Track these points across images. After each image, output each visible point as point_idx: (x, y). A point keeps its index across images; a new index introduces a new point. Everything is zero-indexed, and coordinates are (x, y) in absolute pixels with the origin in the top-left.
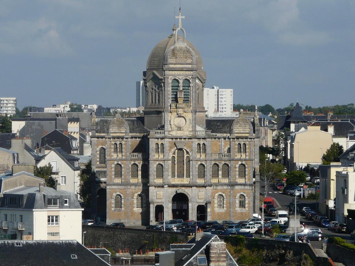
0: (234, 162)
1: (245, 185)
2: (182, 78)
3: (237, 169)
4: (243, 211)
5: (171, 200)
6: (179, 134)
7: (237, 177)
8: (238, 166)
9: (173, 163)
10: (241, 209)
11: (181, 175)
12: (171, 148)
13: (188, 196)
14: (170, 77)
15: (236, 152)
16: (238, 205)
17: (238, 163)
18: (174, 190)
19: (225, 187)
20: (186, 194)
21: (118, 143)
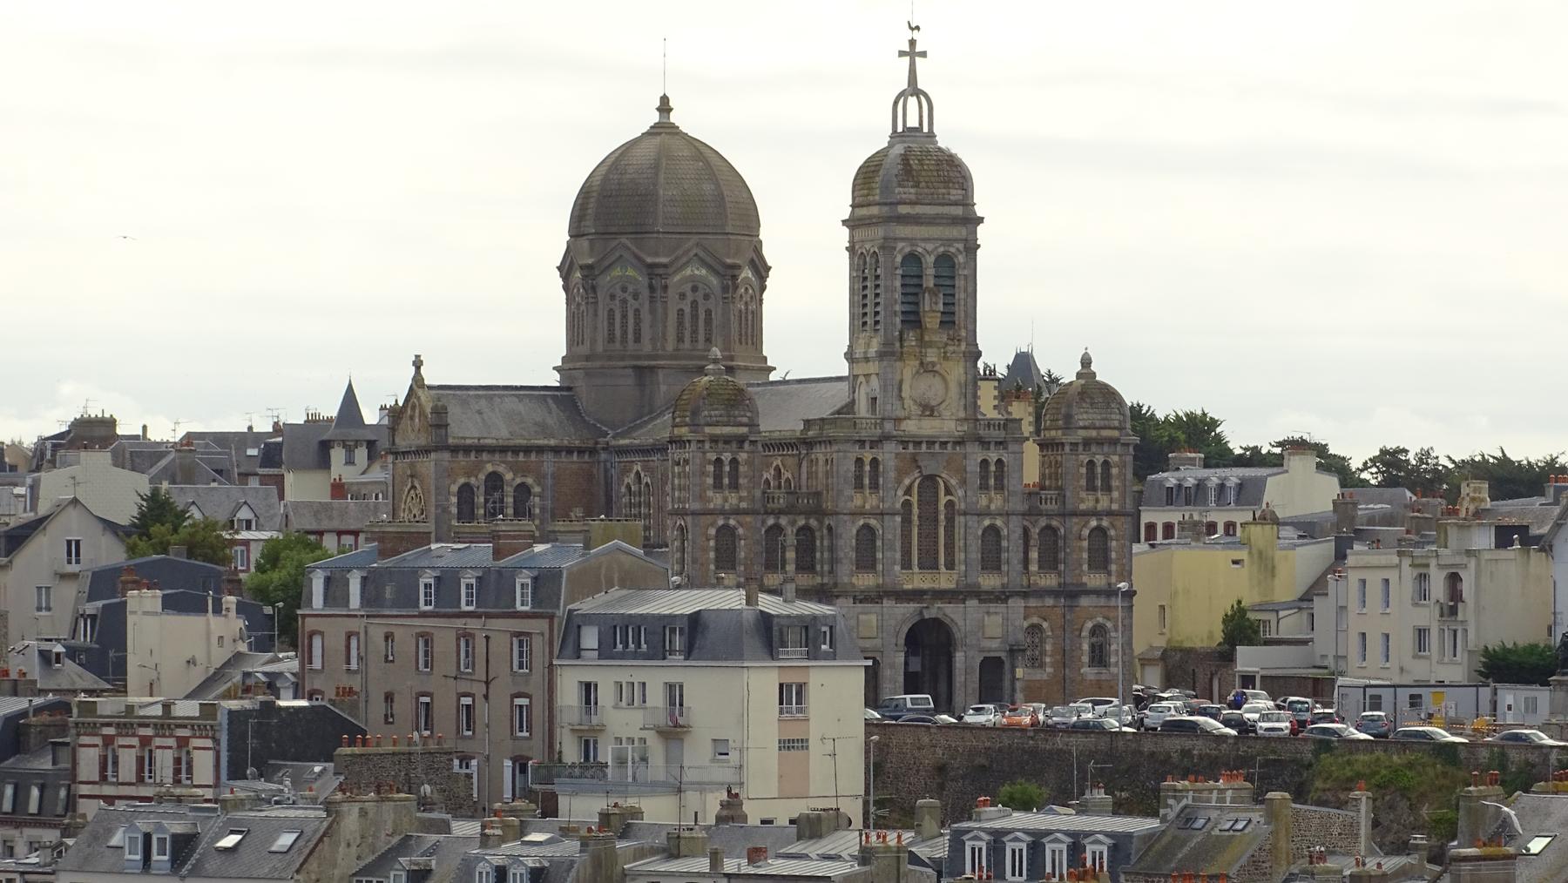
0: (1075, 520)
2: (936, 248)
3: (1085, 544)
5: (902, 641)
6: (928, 427)
7: (1085, 567)
8: (1086, 532)
9: (907, 521)
11: (929, 564)
12: (901, 473)
13: (955, 630)
14: (900, 245)
15: (1081, 487)
16: (1085, 659)
17: (1087, 522)
18: (911, 610)
19: (1050, 602)
20: (947, 621)
21: (727, 457)
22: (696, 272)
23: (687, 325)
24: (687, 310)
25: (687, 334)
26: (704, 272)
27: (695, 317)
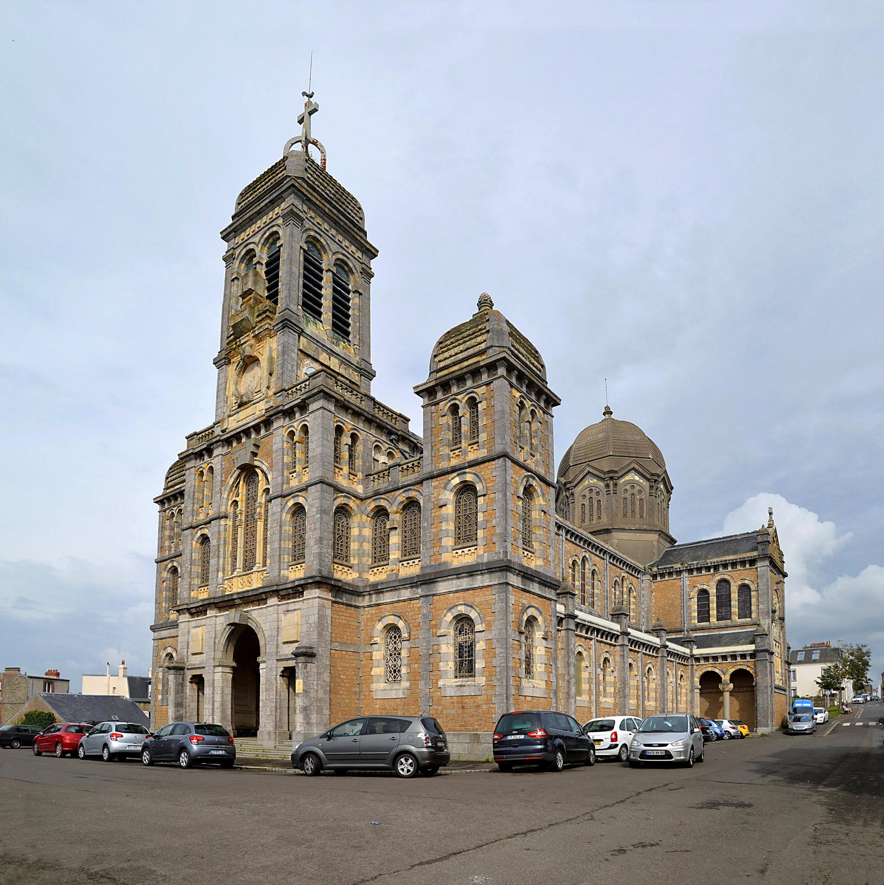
1: (471, 572)
4: (466, 692)
10: (459, 681)
16: (448, 665)
22: (591, 482)
23: (587, 512)
24: (587, 503)
25: (587, 517)
26: (595, 480)
27: (591, 506)
